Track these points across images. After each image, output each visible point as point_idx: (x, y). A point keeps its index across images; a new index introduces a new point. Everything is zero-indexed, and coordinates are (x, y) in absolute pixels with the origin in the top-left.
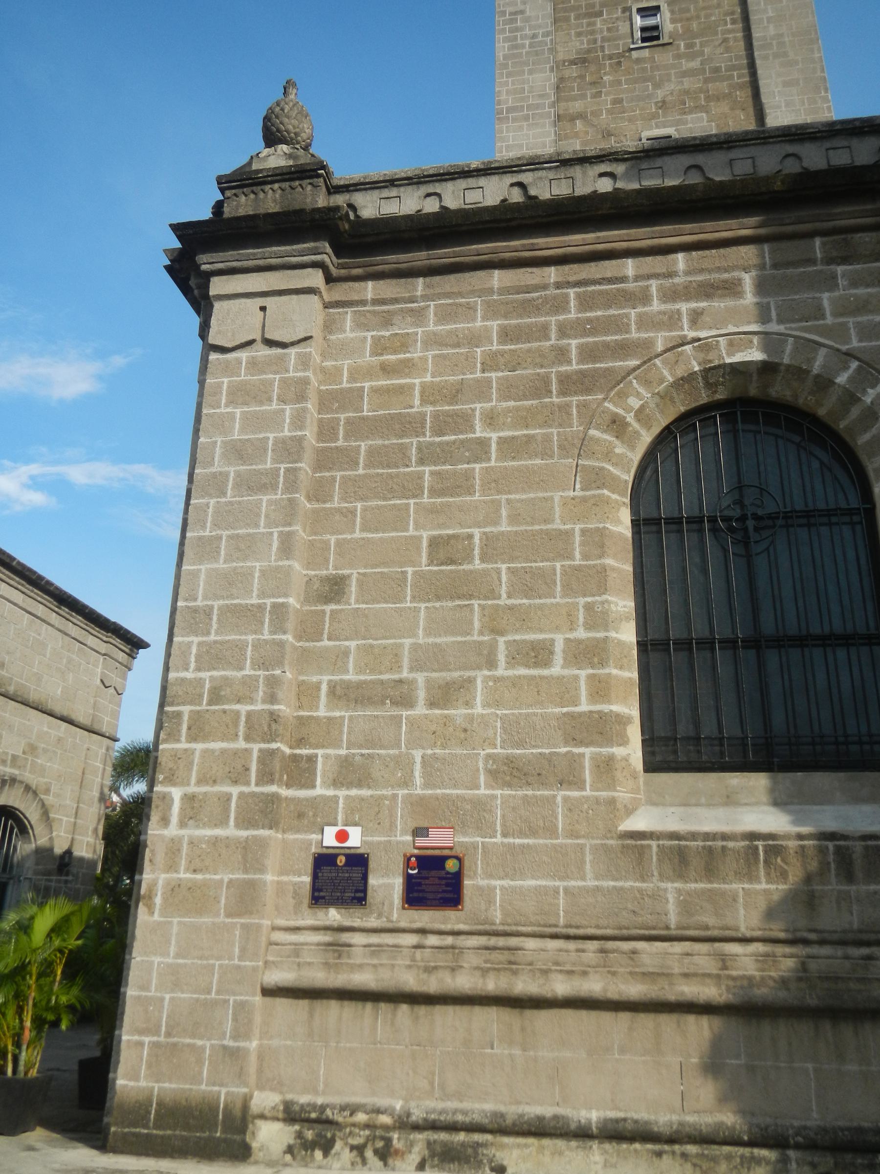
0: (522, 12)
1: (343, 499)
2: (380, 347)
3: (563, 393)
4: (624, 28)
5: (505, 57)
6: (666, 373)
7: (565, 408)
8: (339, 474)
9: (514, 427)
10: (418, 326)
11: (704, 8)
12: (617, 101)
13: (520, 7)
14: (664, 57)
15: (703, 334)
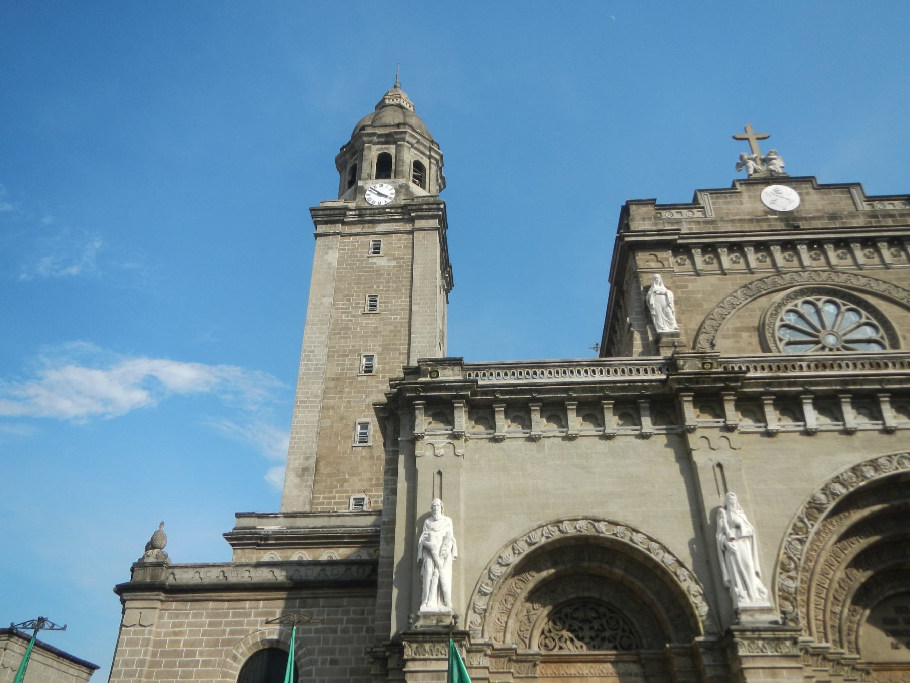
0: (313, 351)
1: (156, 678)
2: (174, 626)
3: (222, 646)
4: (357, 365)
5: (303, 374)
6: (251, 641)
7: (221, 651)
8: (155, 670)
9: (207, 657)
10: (185, 618)
11: (393, 359)
12: (349, 402)
13: (313, 348)
14: (372, 382)
15: (263, 628)
